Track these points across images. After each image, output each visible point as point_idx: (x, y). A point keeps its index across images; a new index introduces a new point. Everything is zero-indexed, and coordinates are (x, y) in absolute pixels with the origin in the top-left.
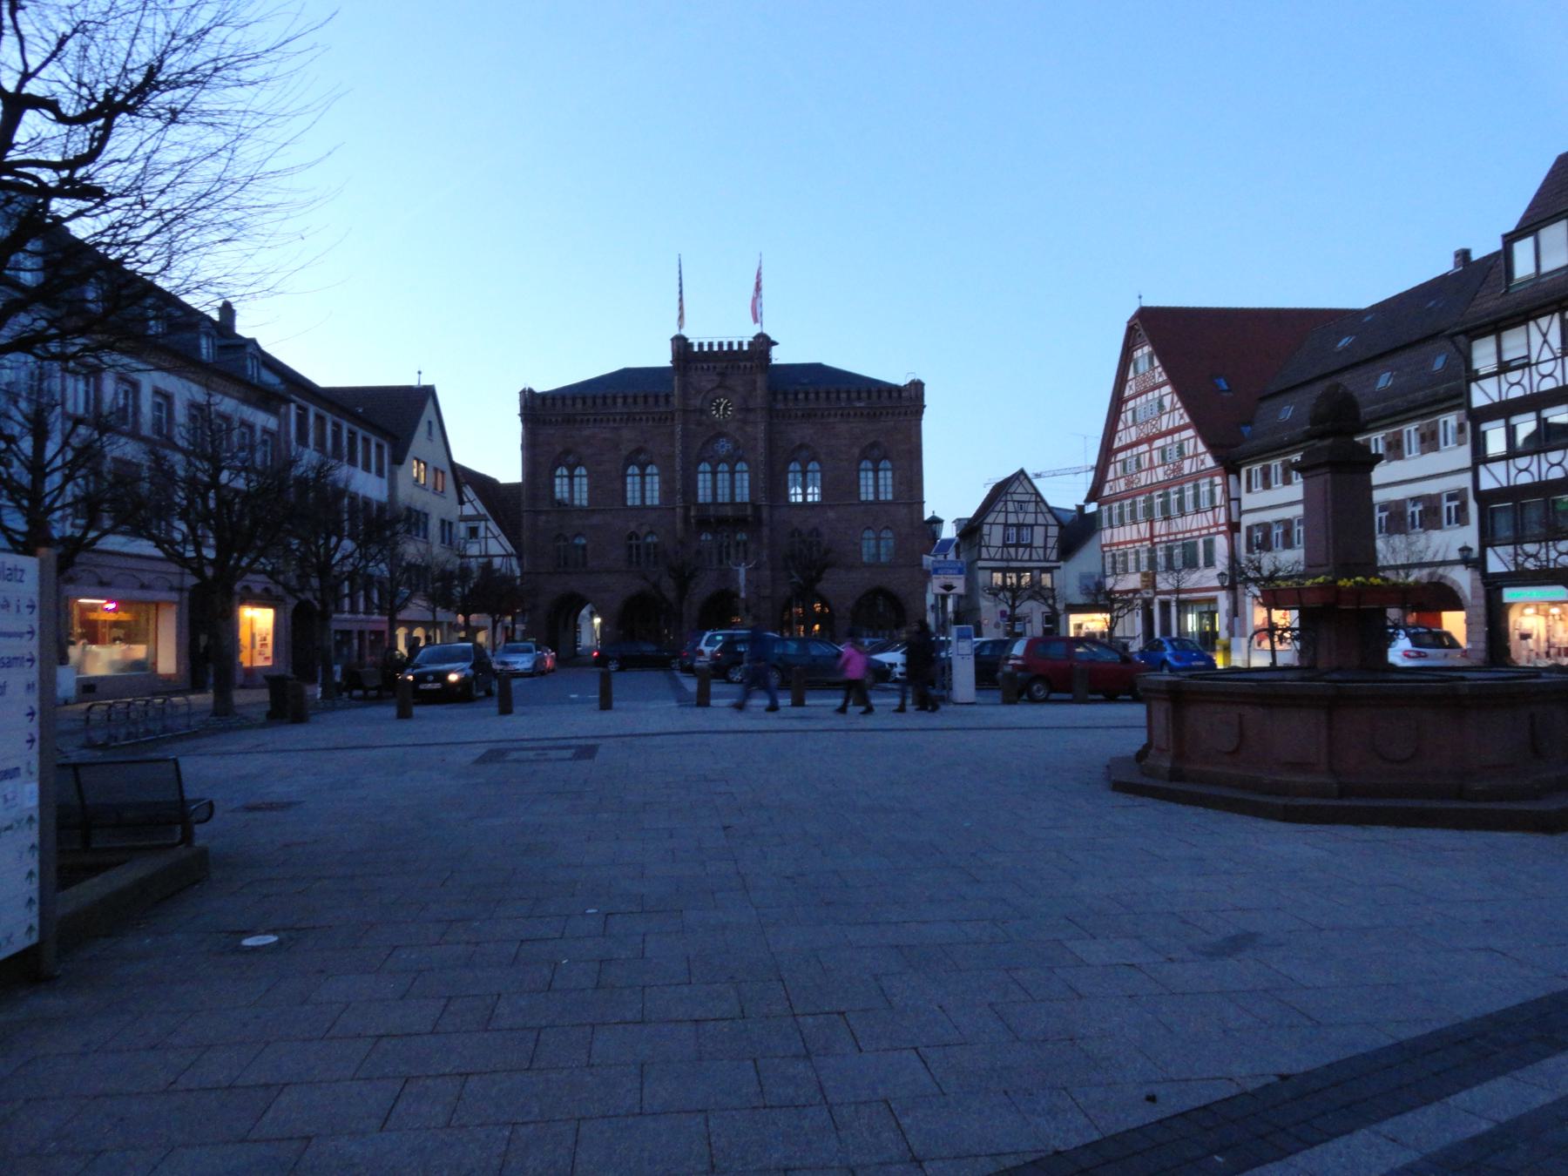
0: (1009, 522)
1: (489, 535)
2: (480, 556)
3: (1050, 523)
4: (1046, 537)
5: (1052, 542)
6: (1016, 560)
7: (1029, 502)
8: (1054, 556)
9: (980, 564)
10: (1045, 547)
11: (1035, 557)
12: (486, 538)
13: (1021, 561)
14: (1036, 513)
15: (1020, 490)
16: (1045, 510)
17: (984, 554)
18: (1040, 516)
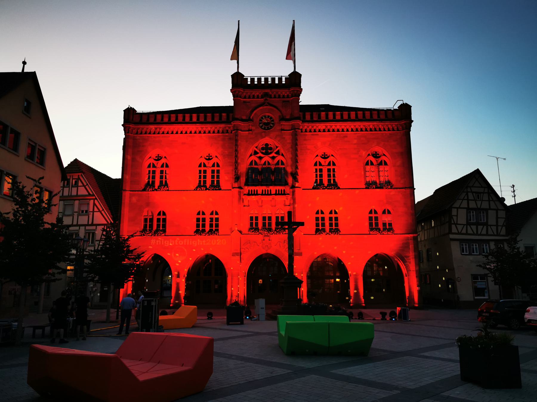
0: (470, 207)
1: (96, 209)
2: (88, 225)
3: (499, 208)
4: (497, 218)
5: (501, 222)
6: (477, 234)
7: (484, 193)
8: (503, 232)
9: (452, 236)
10: (497, 226)
11: (490, 232)
12: (93, 212)
13: (481, 235)
14: (489, 201)
15: (477, 184)
16: (495, 199)
17: (454, 230)
18: (492, 203)
